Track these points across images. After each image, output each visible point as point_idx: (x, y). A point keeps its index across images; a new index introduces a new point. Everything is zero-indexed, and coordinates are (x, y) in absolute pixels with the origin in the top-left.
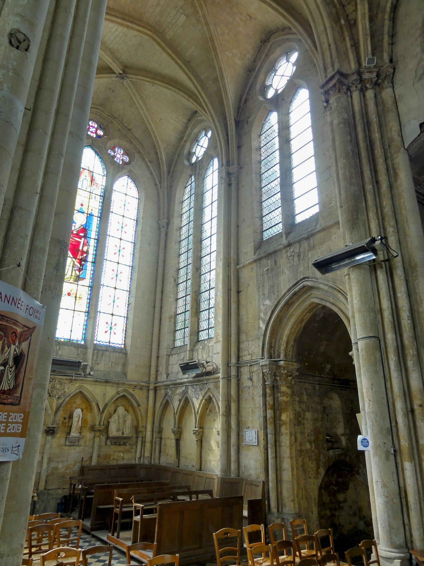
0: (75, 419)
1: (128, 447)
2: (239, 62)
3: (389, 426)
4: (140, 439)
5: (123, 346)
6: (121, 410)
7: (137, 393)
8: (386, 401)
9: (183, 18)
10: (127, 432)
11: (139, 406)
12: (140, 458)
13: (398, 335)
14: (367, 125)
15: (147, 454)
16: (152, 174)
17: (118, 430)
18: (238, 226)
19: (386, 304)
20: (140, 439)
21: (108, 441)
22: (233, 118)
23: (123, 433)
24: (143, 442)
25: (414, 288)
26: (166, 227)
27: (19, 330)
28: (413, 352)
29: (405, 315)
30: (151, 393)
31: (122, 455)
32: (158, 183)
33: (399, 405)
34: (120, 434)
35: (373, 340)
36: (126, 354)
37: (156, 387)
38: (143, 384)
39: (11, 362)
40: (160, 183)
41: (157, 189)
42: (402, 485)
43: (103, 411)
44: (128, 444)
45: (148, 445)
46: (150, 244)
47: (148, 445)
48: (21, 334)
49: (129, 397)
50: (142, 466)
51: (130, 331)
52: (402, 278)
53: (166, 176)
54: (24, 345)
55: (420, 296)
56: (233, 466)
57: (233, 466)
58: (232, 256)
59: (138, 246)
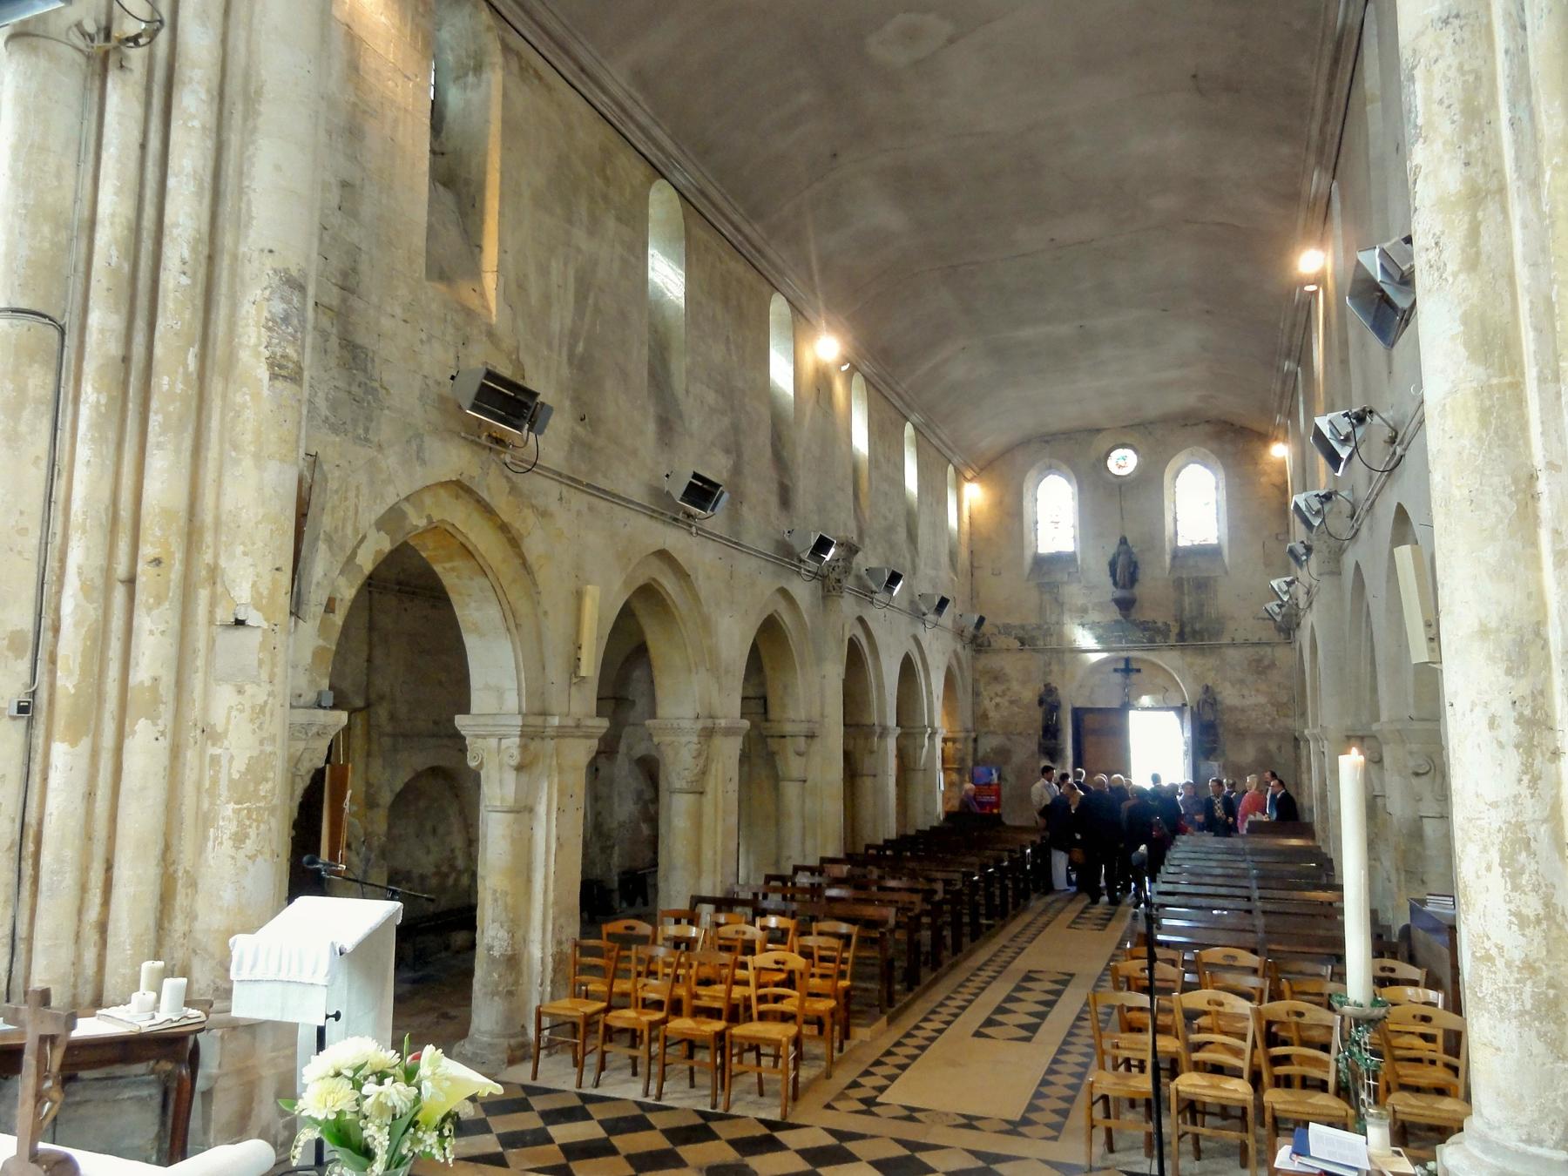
3: (28, 624)
8: (33, 540)
13: (141, 324)
19: (112, 204)
25: (240, 174)
28: (172, 384)
29: (179, 250)
33: (80, 555)
35: (23, 323)
42: (32, 818)
52: (196, 123)
55: (249, 203)
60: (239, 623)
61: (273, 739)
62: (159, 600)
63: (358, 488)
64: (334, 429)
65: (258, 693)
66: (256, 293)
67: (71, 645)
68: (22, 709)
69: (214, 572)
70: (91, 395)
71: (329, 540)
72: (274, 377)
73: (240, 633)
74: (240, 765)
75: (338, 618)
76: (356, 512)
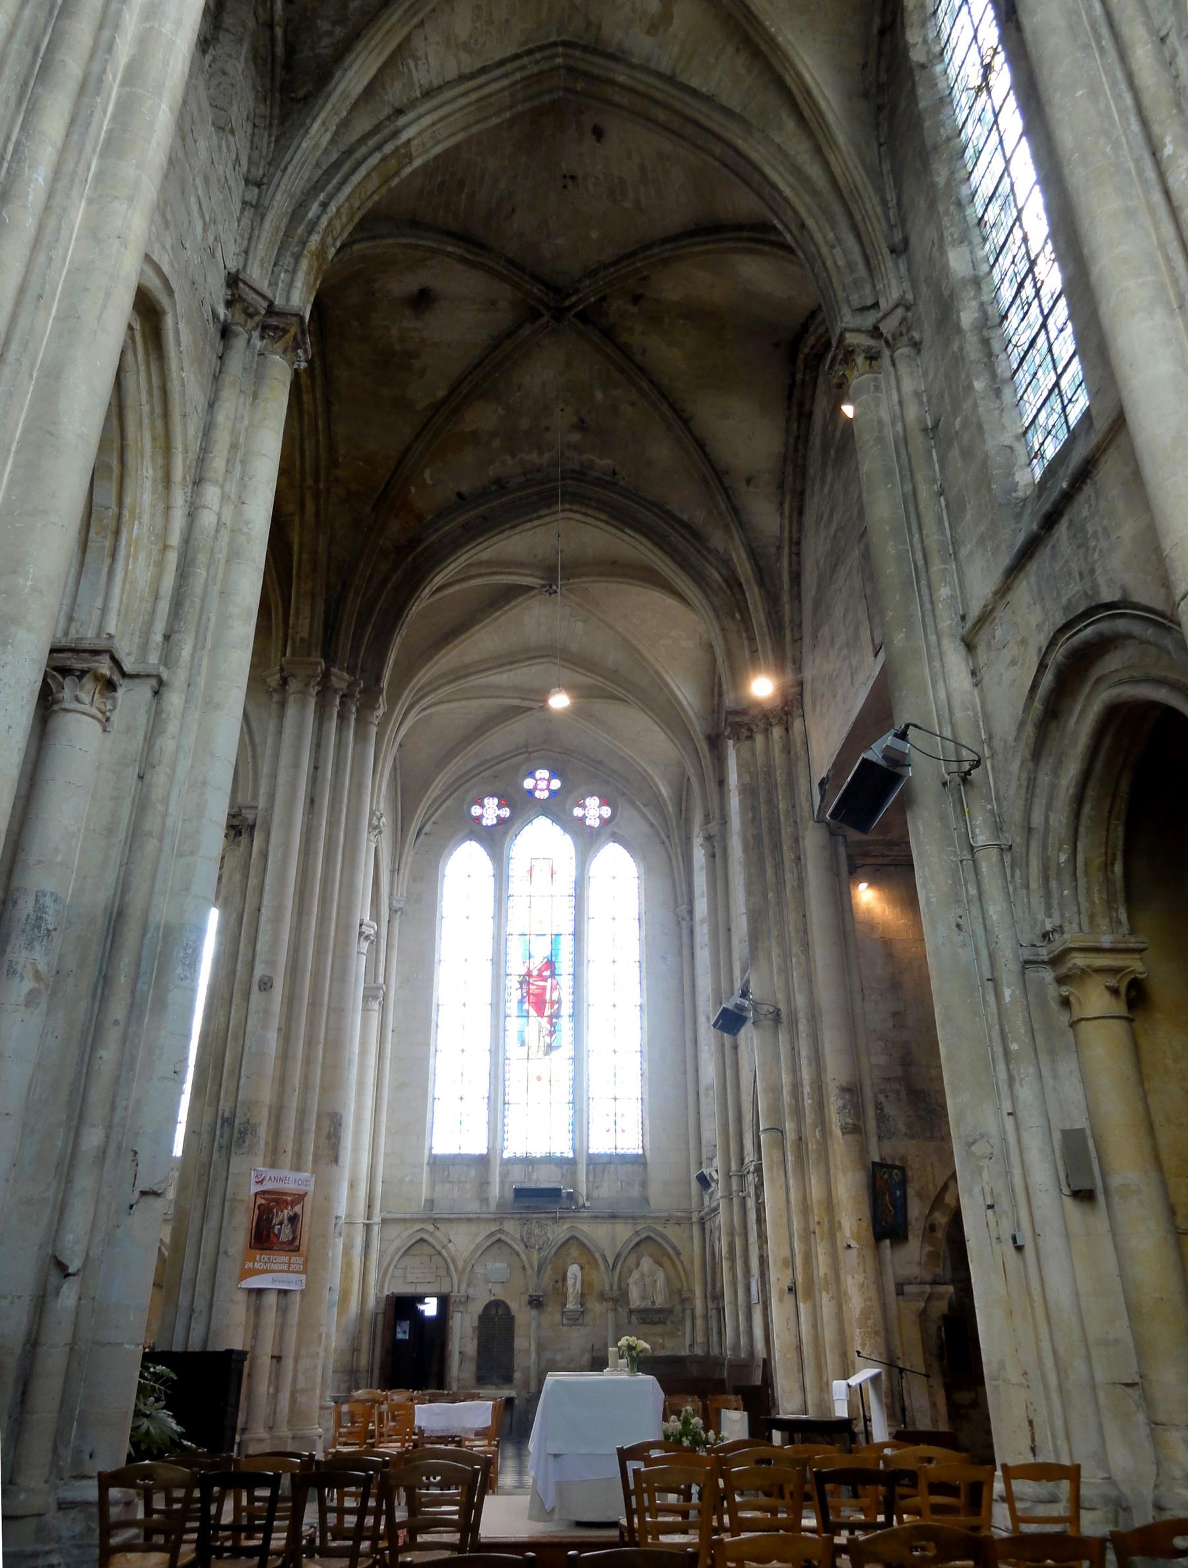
0: (570, 1282)
1: (669, 1327)
2: (689, 644)
4: (688, 1312)
5: (641, 1152)
6: (646, 1263)
7: (672, 1232)
8: (785, 1220)
9: (580, 626)
10: (660, 1301)
11: (678, 1254)
12: (692, 1346)
14: (771, 789)
15: (700, 1338)
16: (652, 825)
17: (644, 1298)
18: (729, 930)
19: (786, 1079)
20: (688, 1312)
21: (633, 1317)
22: (701, 737)
23: (653, 1303)
24: (693, 1318)
26: (688, 918)
27: (289, 1199)
30: (696, 1230)
31: (661, 1341)
32: (665, 839)
34: (647, 1304)
36: (645, 1164)
37: (702, 1218)
38: (679, 1214)
39: (286, 1222)
40: (668, 837)
41: (667, 849)
43: (614, 1266)
44: (668, 1322)
45: (699, 1322)
46: (664, 958)
47: (699, 1322)
48: (292, 1201)
49: (659, 1239)
50: (694, 1359)
51: (647, 1123)
53: (675, 824)
54: (297, 1209)
56: (743, 1340)
57: (743, 1340)
58: (723, 986)
59: (644, 965)
60: (849, 1246)
61: (870, 1299)
62: (822, 1240)
63: (932, 1164)
64: (911, 1137)
65: (860, 1278)
66: (832, 1099)
67: (799, 1261)
68: (790, 1290)
69: (840, 1223)
70: (790, 1158)
71: (919, 1194)
72: (843, 1134)
73: (850, 1251)
74: (858, 1312)
75: (940, 1234)
76: (934, 1177)
